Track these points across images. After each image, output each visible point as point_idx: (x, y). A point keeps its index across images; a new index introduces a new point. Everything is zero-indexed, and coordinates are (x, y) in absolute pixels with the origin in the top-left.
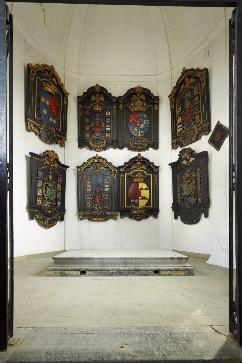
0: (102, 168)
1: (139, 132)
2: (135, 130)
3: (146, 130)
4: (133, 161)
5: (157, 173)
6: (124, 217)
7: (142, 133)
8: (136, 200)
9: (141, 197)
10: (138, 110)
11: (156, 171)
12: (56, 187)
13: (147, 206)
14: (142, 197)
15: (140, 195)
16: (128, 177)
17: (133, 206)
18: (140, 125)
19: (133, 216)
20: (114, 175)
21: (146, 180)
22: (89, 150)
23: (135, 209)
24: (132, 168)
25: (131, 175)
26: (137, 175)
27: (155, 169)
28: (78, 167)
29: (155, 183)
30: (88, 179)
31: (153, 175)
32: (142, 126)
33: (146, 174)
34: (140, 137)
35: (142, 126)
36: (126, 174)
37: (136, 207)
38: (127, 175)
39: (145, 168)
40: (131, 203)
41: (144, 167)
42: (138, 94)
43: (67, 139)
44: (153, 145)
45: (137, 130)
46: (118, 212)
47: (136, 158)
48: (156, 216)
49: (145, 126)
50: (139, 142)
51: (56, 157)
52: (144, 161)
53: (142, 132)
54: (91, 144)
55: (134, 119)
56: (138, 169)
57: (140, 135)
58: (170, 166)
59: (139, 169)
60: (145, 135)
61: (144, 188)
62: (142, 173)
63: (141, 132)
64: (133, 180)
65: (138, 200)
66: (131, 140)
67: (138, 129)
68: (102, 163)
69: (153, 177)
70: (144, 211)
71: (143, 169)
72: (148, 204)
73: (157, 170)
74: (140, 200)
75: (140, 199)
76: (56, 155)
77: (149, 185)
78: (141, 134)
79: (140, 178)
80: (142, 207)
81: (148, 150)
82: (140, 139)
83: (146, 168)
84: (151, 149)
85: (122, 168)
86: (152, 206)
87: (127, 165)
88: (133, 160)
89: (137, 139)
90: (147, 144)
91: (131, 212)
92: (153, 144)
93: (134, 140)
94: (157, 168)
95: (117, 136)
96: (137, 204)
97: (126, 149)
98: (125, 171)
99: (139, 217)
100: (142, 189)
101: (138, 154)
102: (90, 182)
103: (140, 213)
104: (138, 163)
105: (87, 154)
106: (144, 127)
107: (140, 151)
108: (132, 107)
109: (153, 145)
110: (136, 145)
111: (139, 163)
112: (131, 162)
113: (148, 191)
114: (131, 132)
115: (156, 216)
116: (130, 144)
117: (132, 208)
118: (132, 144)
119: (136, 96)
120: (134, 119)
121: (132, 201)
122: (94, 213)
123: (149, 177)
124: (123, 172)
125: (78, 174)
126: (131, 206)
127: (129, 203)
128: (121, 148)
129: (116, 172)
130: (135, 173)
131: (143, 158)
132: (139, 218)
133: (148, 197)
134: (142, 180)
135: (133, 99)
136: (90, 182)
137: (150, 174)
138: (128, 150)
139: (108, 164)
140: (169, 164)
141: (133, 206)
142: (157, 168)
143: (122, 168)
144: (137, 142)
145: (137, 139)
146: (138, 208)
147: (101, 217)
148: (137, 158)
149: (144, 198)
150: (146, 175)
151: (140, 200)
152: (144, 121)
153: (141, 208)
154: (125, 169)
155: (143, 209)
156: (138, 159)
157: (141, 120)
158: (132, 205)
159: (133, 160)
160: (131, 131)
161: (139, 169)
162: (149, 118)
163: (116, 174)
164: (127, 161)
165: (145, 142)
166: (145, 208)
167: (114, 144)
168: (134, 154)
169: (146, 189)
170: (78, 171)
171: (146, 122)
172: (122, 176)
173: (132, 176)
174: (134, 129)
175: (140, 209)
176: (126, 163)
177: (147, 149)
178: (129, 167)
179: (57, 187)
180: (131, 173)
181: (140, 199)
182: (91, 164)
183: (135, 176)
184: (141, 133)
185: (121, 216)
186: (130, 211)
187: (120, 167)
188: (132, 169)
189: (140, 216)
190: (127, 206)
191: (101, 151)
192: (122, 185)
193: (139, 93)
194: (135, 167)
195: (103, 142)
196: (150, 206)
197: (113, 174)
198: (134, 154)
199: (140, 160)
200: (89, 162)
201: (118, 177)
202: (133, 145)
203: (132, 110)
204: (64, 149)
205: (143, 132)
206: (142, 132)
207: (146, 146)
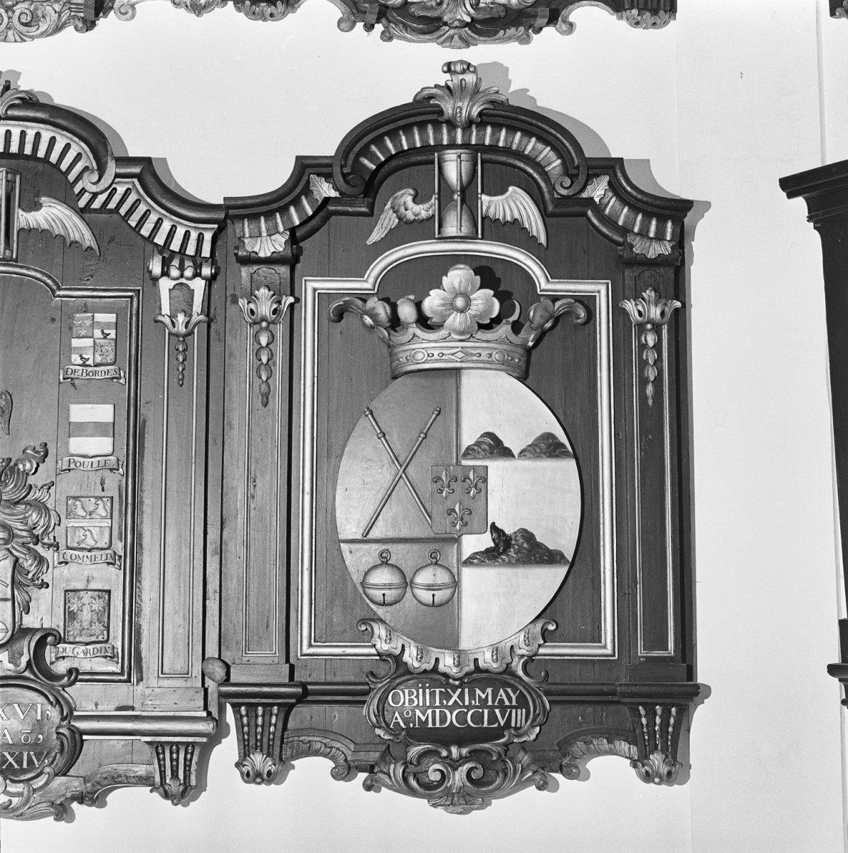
5: (671, 276)
9: (485, 541)
11: (656, 250)
15: (471, 516)
20: (183, 292)
21: (548, 355)
24: (387, 221)
27: (643, 234)
29: (643, 382)
31: (616, 298)
33: (544, 283)
36: (312, 286)
37: (435, 652)
39: (535, 224)
47: (421, 111)
48: (656, 759)
52: (516, 137)
58: (800, 204)
59: (465, 230)
65: (442, 577)
69: (619, 314)
70: (522, 702)
71: (511, 231)
73: (660, 237)
74: (468, 574)
86: (608, 645)
88: (393, 134)
94: (662, 221)
96: (441, 623)
99: (454, 764)
100: (495, 447)
101: (449, 68)
103: (478, 718)
111: (466, 166)
113: (569, 467)
115: (656, 759)
123: (572, 323)
139: (112, 169)
140: (792, 185)
142: (662, 221)
146: (447, 662)
149: (515, 549)
151: (468, 574)
153: (486, 660)
156: (452, 125)
159: (393, 134)
161: (465, 230)
164: (327, 147)
169: (547, 447)
175: (477, 677)
176: (306, 167)
185: (245, 751)
188: (376, 236)
189: (473, 755)
191: (45, 34)
196: (596, 637)
197: (165, 285)
198: (405, 68)
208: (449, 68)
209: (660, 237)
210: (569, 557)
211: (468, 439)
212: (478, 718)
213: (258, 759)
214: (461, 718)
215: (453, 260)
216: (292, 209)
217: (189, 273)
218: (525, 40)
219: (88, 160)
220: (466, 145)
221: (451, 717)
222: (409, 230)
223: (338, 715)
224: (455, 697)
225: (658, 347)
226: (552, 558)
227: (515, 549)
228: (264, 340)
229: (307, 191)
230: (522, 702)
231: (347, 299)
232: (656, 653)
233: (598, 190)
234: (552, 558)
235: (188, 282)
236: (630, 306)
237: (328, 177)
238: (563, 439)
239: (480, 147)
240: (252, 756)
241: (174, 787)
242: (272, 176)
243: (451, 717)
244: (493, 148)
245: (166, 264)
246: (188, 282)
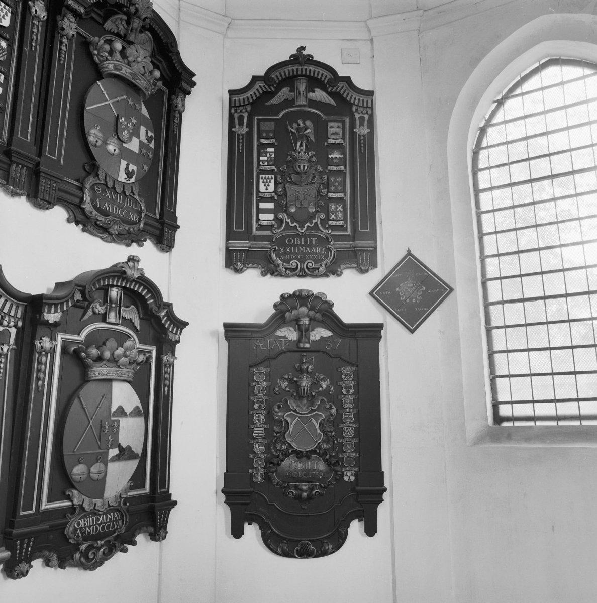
7: (130, 170)
10: (130, 78)
13: (132, 488)
27: (172, 332)
34: (124, 185)
36: (60, 336)
39: (137, 322)
41: (131, 314)
42: (136, 23)
47: (117, 273)
50: (119, 206)
53: (132, 167)
55: (109, 102)
57: (122, 177)
61: (128, 410)
63: (128, 165)
72: (137, 480)
74: (110, 465)
75: (115, 459)
78: (129, 175)
83: (140, 319)
85: (56, 305)
96: (97, 486)
97: (59, 213)
100: (121, 412)
108: (111, 52)
113: (141, 420)
117: (72, 509)
119: (124, 22)
120: (109, 102)
121: (78, 471)
124: (56, 324)
126: (69, 498)
135: (108, 25)
138: (69, 221)
143: (56, 305)
144: (113, 202)
148: (124, 273)
149: (125, 454)
162: (155, 125)
165: (140, 213)
174: (105, 143)
178: (83, 306)
181: (115, 459)
192: (39, 393)
193: (139, 17)
202: (95, 207)
203: (111, 67)
205: (135, 168)
206: (132, 167)
210: (140, 455)
211: (114, 408)
214: (103, 528)
216: (65, 303)
217: (12, 324)
220: (120, 287)
221: (99, 528)
224: (101, 519)
231: (80, 346)
232: (162, 490)
235: (9, 329)
240: (20, 565)
244: (129, 289)
246: (9, 329)
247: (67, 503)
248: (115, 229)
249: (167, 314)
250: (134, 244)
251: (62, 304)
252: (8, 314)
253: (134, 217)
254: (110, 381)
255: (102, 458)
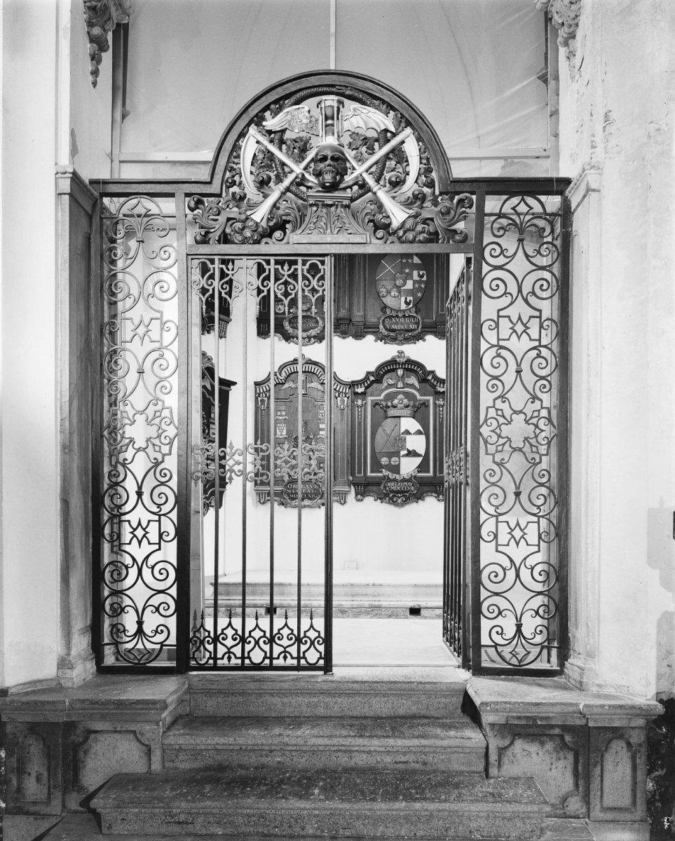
0: (312, 385)
1: (403, 299)
2: (392, 294)
3: (419, 295)
4: (388, 368)
6: (364, 497)
7: (408, 301)
8: (393, 459)
9: (406, 452)
11: (442, 390)
12: (207, 431)
14: (408, 450)
15: (403, 447)
16: (375, 404)
17: (385, 472)
18: (405, 284)
19: (386, 495)
21: (419, 412)
22: (284, 341)
23: (390, 480)
25: (381, 400)
26: (396, 401)
27: (440, 386)
28: (257, 384)
29: (440, 417)
30: (280, 411)
31: (434, 400)
32: (409, 285)
33: (419, 397)
34: (404, 311)
35: (409, 285)
36: (370, 399)
37: (395, 475)
38: (372, 401)
39: (417, 384)
40: (382, 467)
43: (231, 320)
44: (435, 330)
45: (397, 294)
46: (350, 487)
47: (393, 362)
49: (417, 286)
51: (209, 365)
54: (288, 328)
56: (399, 386)
57: (403, 306)
60: (415, 305)
61: (412, 431)
62: (407, 395)
63: (406, 299)
64: (385, 411)
65: (397, 459)
66: (382, 319)
67: (400, 293)
68: (313, 373)
69: (435, 404)
70: (413, 485)
71: (412, 386)
72: (423, 467)
73: (443, 387)
75: (403, 456)
76: (209, 359)
77: (424, 422)
78: (407, 303)
79: (402, 409)
80: (407, 474)
81: (424, 340)
82: (404, 316)
83: (419, 382)
84: (430, 338)
85: (361, 384)
86: (431, 474)
87: (372, 378)
89: (397, 316)
90: (420, 327)
91: (382, 487)
92: (436, 328)
93: (390, 317)
95: (350, 310)
96: (396, 469)
97: (370, 338)
98: (369, 390)
99: (399, 498)
100: (407, 432)
102: (284, 417)
103: (404, 488)
104: (400, 372)
105: (280, 351)
106: (414, 286)
107: (403, 344)
109: (435, 330)
110: (393, 331)
111: (402, 372)
112: (381, 370)
113: (423, 437)
114: (384, 300)
116: (381, 327)
118: (385, 327)
121: (384, 460)
122: (292, 489)
123: (425, 405)
124: (362, 393)
125: (256, 398)
126: (381, 472)
127: (377, 466)
128: (359, 336)
129: (346, 394)
130: (391, 397)
131: (409, 361)
132: (400, 500)
133: (422, 451)
134: (408, 411)
136: (284, 417)
137: (428, 398)
138: (376, 341)
141: (385, 472)
143: (361, 384)
144: (397, 323)
145: (397, 316)
147: (310, 499)
148: (396, 361)
149: (412, 454)
150: (417, 401)
152: (415, 273)
154: (367, 388)
155: (411, 478)
156: (399, 364)
157: (407, 271)
158: (384, 470)
160: (384, 297)
161: (402, 386)
163: (346, 399)
164: (373, 369)
165: (417, 323)
166: (415, 477)
167: (343, 328)
168: (387, 351)
169: (419, 432)
170: (258, 391)
171: (419, 275)
172: (360, 402)
173: (384, 404)
174: (389, 292)
175: (404, 480)
176: (368, 373)
177: (421, 339)
179: (209, 432)
180: (382, 397)
181: (403, 456)
182: (288, 376)
183: (389, 404)
184: (406, 302)
185: (357, 495)
186: (379, 484)
187: (353, 384)
188: (383, 387)
190: (372, 472)
194: (391, 382)
195: (317, 322)
196: (429, 472)
198: (387, 351)
199: (402, 365)
200: (283, 373)
201: (353, 406)
202: (387, 329)
204: (226, 341)
205: (411, 298)
207: (417, 332)
208: (398, 352)
209: (443, 387)
211: (402, 430)
212: (404, 488)
213: (359, 496)
214: (401, 488)
215: (398, 393)
218: (415, 343)
219: (322, 372)
221: (399, 488)
222: (390, 386)
223: (375, 488)
225: (443, 411)
226: (420, 455)
227: (412, 454)
228: (360, 410)
229: (369, 379)
230: (413, 485)
233: (430, 378)
234: (420, 455)
236: (437, 402)
237: (373, 376)
238: (422, 430)
239: (405, 368)
241: (342, 502)
242: (361, 376)
243: (399, 488)
245: (339, 394)
247: (380, 475)
248: (401, 338)
249: (433, 377)
250: (421, 341)
251: (364, 383)
252: (342, 392)
253: (414, 326)
254: (399, 417)
255: (397, 454)
